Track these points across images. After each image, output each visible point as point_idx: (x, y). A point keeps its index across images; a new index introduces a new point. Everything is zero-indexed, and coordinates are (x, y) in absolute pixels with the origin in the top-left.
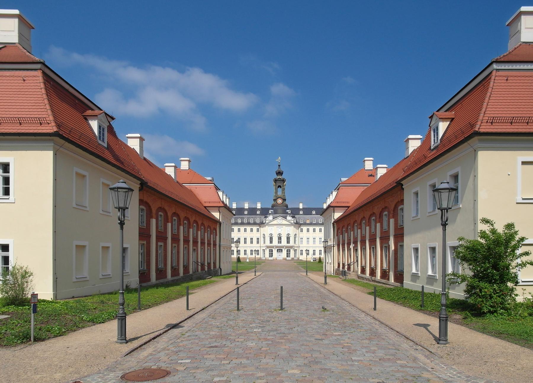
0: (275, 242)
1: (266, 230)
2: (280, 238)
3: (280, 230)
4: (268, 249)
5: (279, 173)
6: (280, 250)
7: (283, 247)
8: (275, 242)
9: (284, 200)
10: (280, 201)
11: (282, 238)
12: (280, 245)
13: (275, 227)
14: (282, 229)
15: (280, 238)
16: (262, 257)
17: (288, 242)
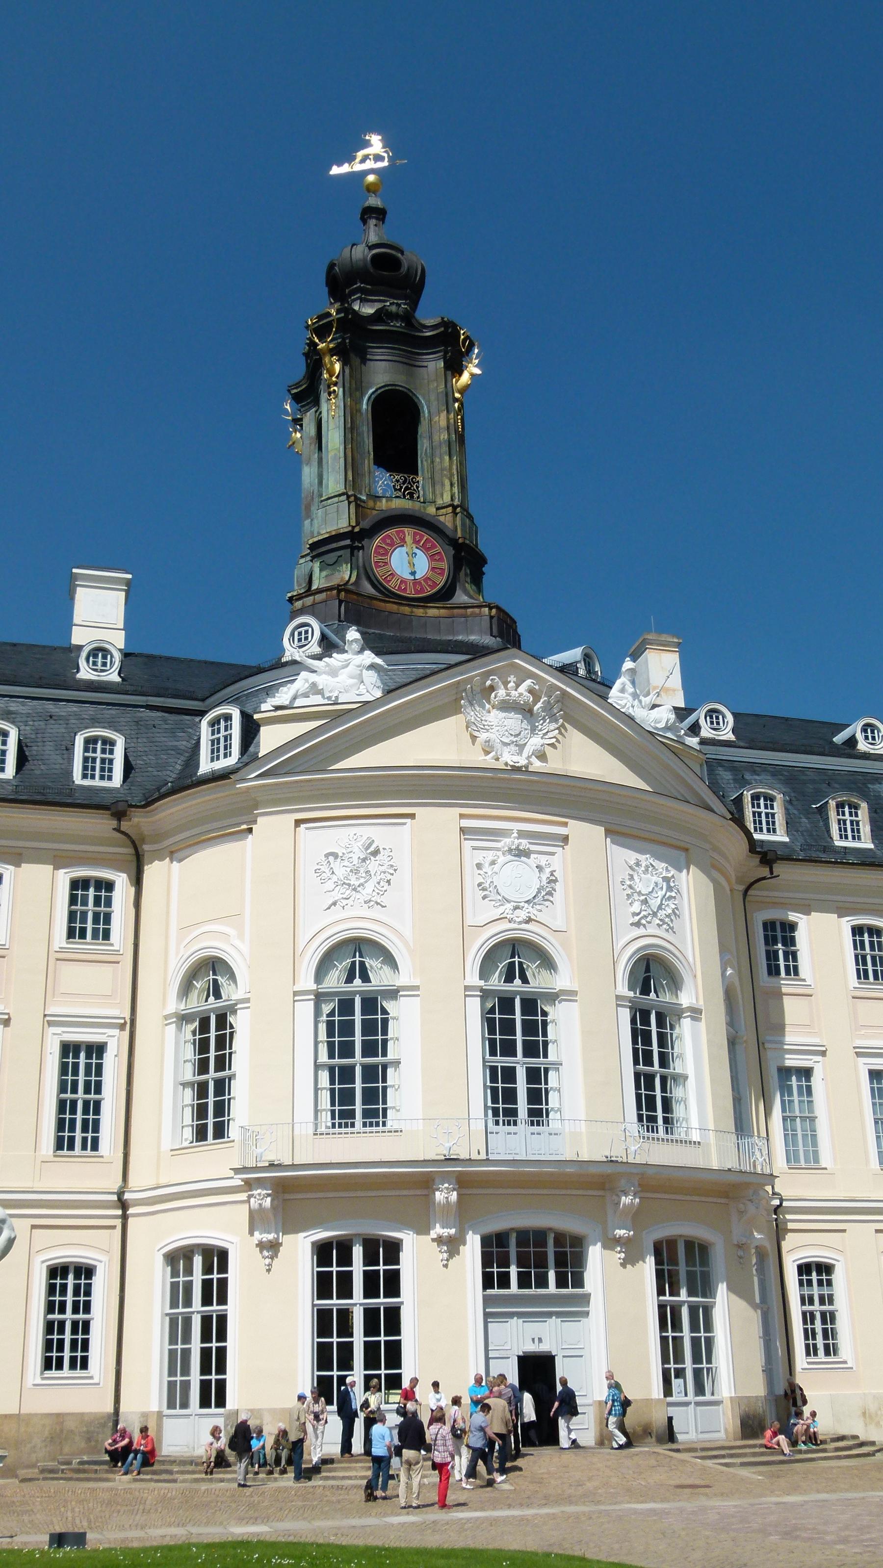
0: (436, 1101)
1: (251, 897)
2: (515, 1027)
3: (518, 879)
4: (299, 1249)
5: (389, 272)
6: (531, 1260)
7: (596, 1183)
8: (436, 1101)
9: (467, 561)
10: (409, 562)
11: (565, 1027)
12: (518, 1144)
13: (440, 820)
14: (558, 861)
15: (515, 1027)
16: (145, 1395)
17: (654, 1100)
